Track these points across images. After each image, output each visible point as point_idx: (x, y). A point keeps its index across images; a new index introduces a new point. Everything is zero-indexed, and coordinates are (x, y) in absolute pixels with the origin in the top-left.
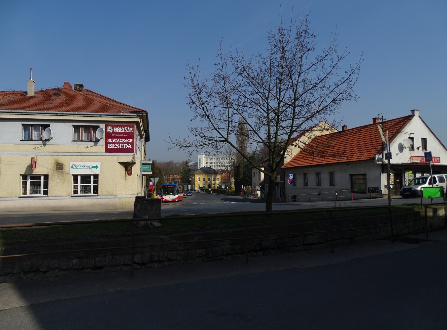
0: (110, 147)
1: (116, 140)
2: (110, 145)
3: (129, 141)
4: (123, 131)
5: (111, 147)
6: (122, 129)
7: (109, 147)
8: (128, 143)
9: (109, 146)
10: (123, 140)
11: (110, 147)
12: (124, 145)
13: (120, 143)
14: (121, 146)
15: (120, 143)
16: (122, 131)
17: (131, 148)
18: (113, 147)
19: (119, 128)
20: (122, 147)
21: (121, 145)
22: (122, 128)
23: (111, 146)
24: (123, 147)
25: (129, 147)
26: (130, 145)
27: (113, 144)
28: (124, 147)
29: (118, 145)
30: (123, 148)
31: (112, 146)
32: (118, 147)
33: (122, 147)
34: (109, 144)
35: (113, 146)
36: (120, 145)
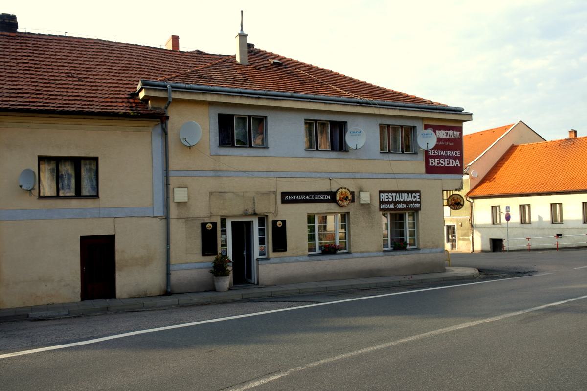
0: (432, 164)
1: (439, 151)
2: (432, 160)
3: (456, 153)
4: (448, 137)
5: (433, 165)
6: (447, 133)
7: (431, 165)
8: (455, 158)
9: (431, 162)
10: (449, 153)
11: (432, 164)
12: (451, 160)
13: (444, 157)
14: (446, 162)
15: (444, 157)
16: (446, 136)
17: (459, 166)
18: (436, 165)
19: (442, 131)
20: (448, 164)
21: (446, 160)
22: (447, 131)
23: (433, 162)
24: (449, 164)
25: (457, 165)
26: (457, 160)
27: (436, 160)
28: (451, 165)
29: (442, 161)
30: (449, 165)
31: (435, 162)
32: (442, 164)
33: (448, 164)
34: (431, 159)
35: (436, 162)
36: (444, 161)
